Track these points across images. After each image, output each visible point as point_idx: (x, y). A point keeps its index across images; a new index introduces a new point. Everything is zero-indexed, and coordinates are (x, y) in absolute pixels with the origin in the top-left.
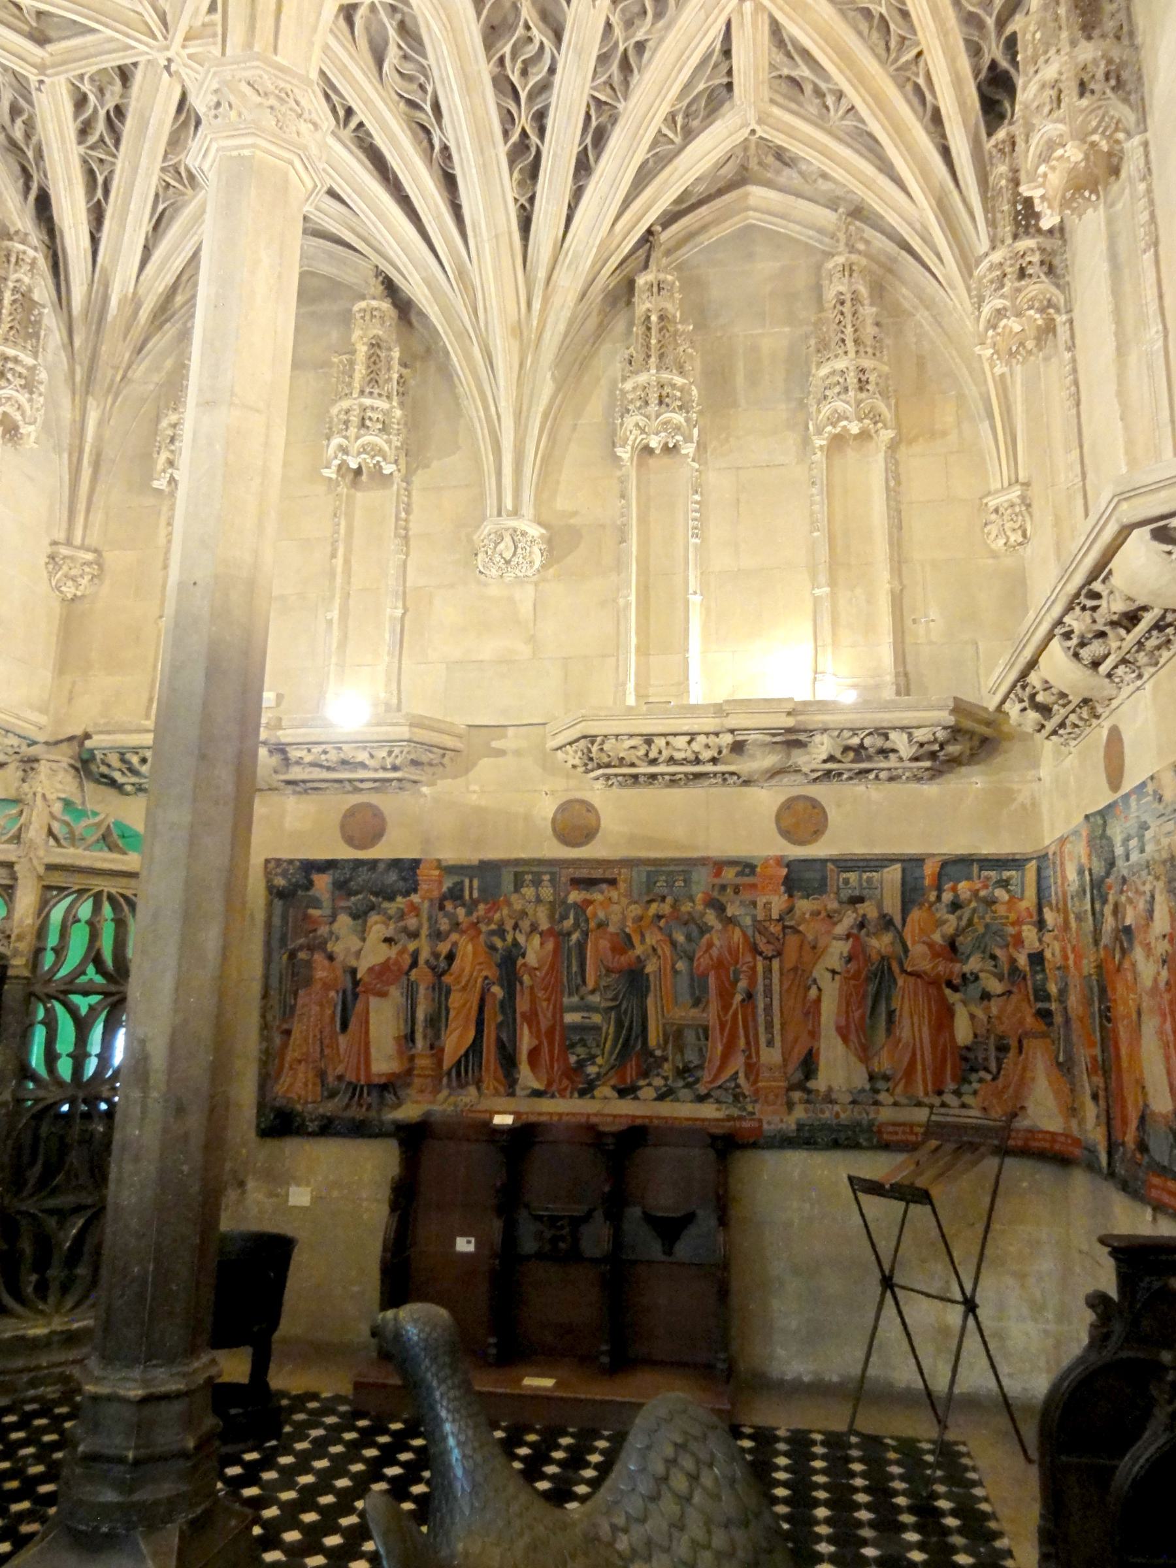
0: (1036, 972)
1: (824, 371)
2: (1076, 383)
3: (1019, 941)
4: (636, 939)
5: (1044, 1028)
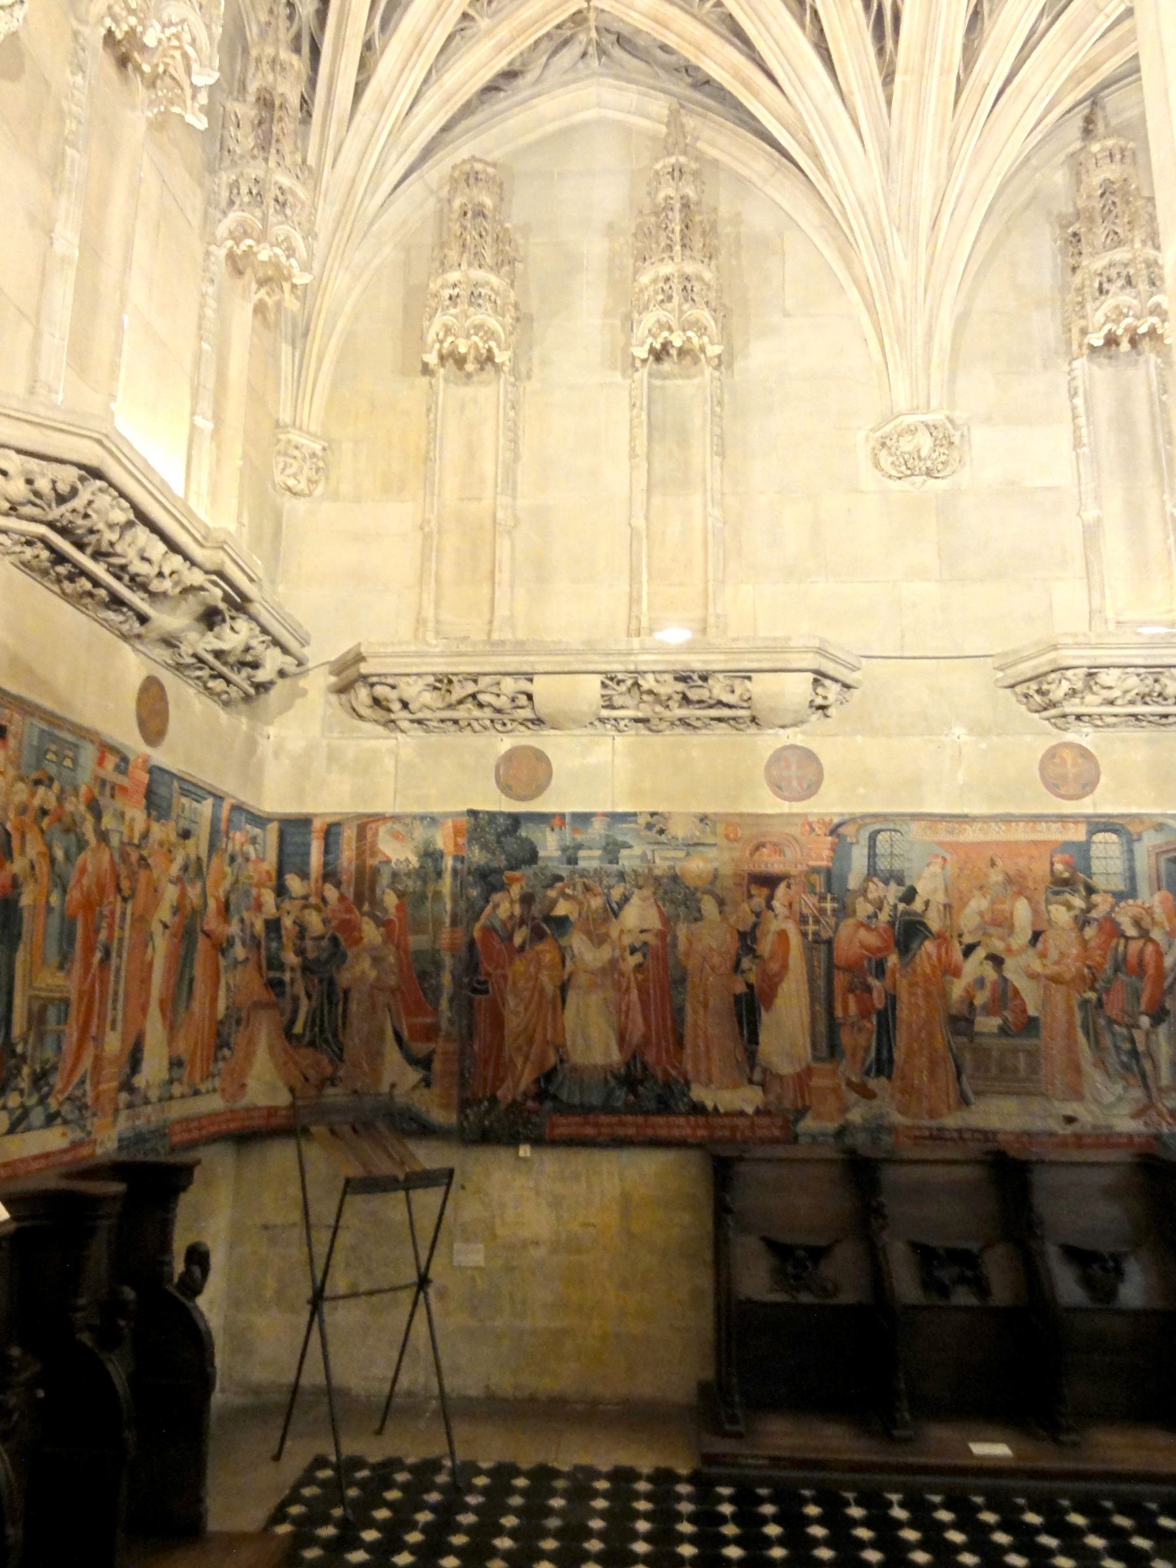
0: (272, 940)
3: (259, 906)
4: (15, 844)
5: (273, 997)
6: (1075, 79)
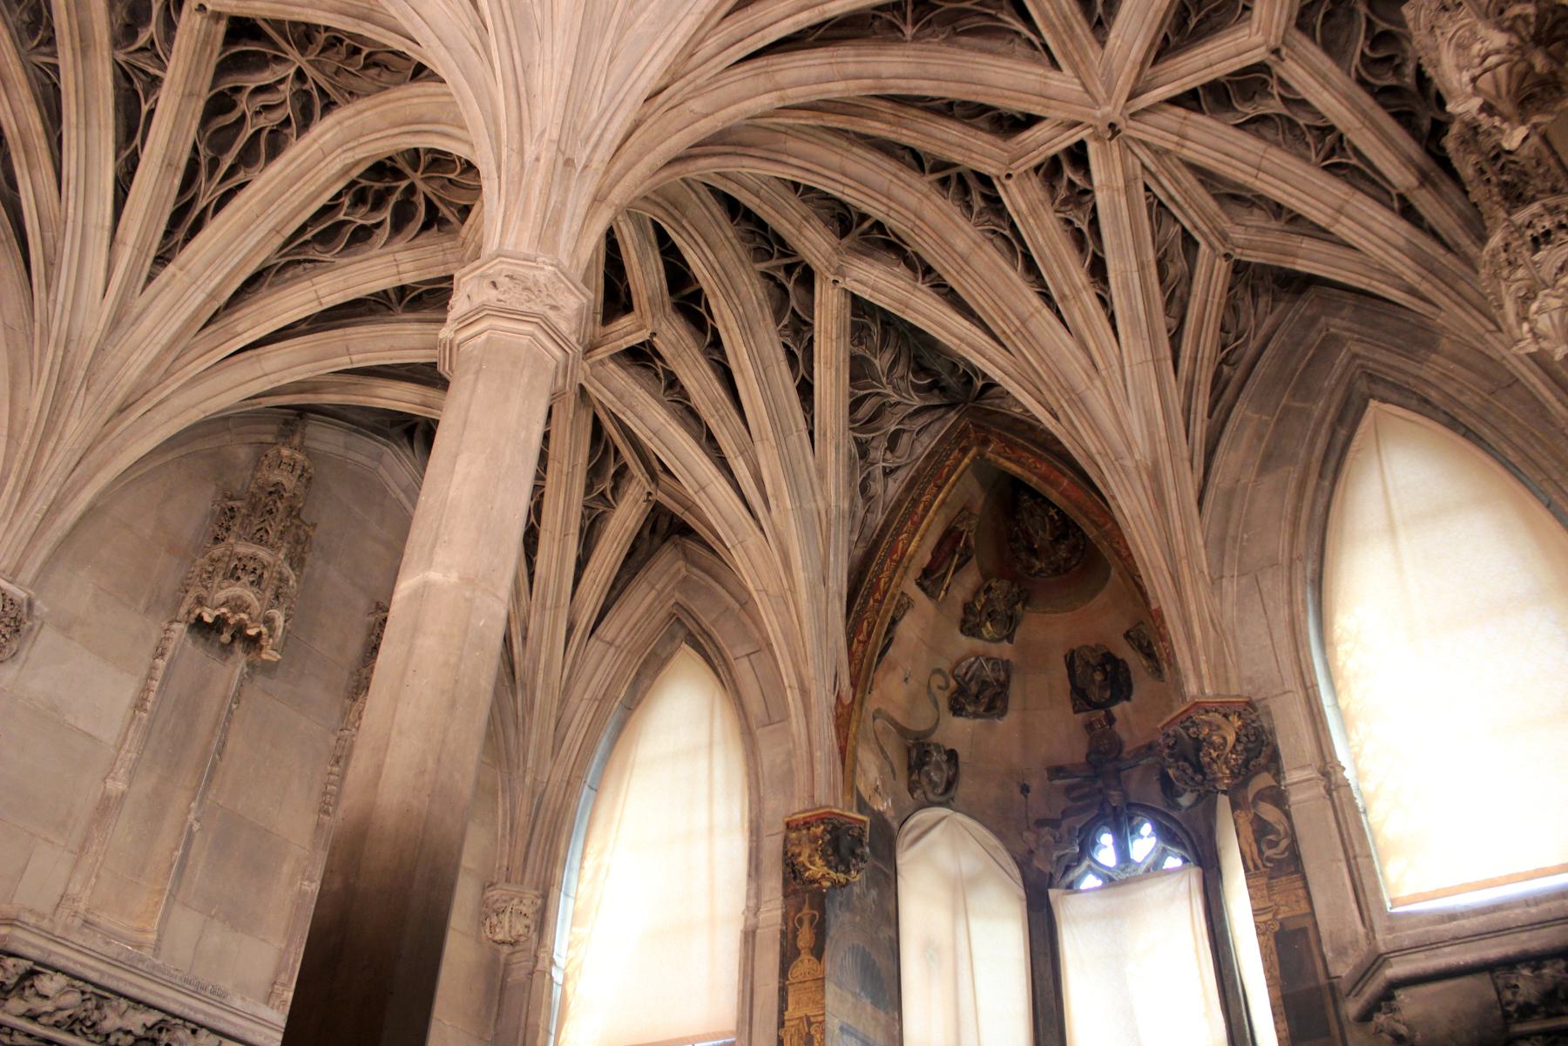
6: (300, 387)
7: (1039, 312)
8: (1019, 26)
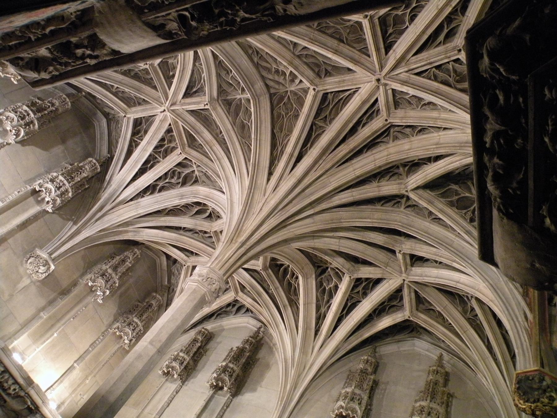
1: (136, 320)
2: (171, 402)
7: (440, 136)
8: (347, 93)
